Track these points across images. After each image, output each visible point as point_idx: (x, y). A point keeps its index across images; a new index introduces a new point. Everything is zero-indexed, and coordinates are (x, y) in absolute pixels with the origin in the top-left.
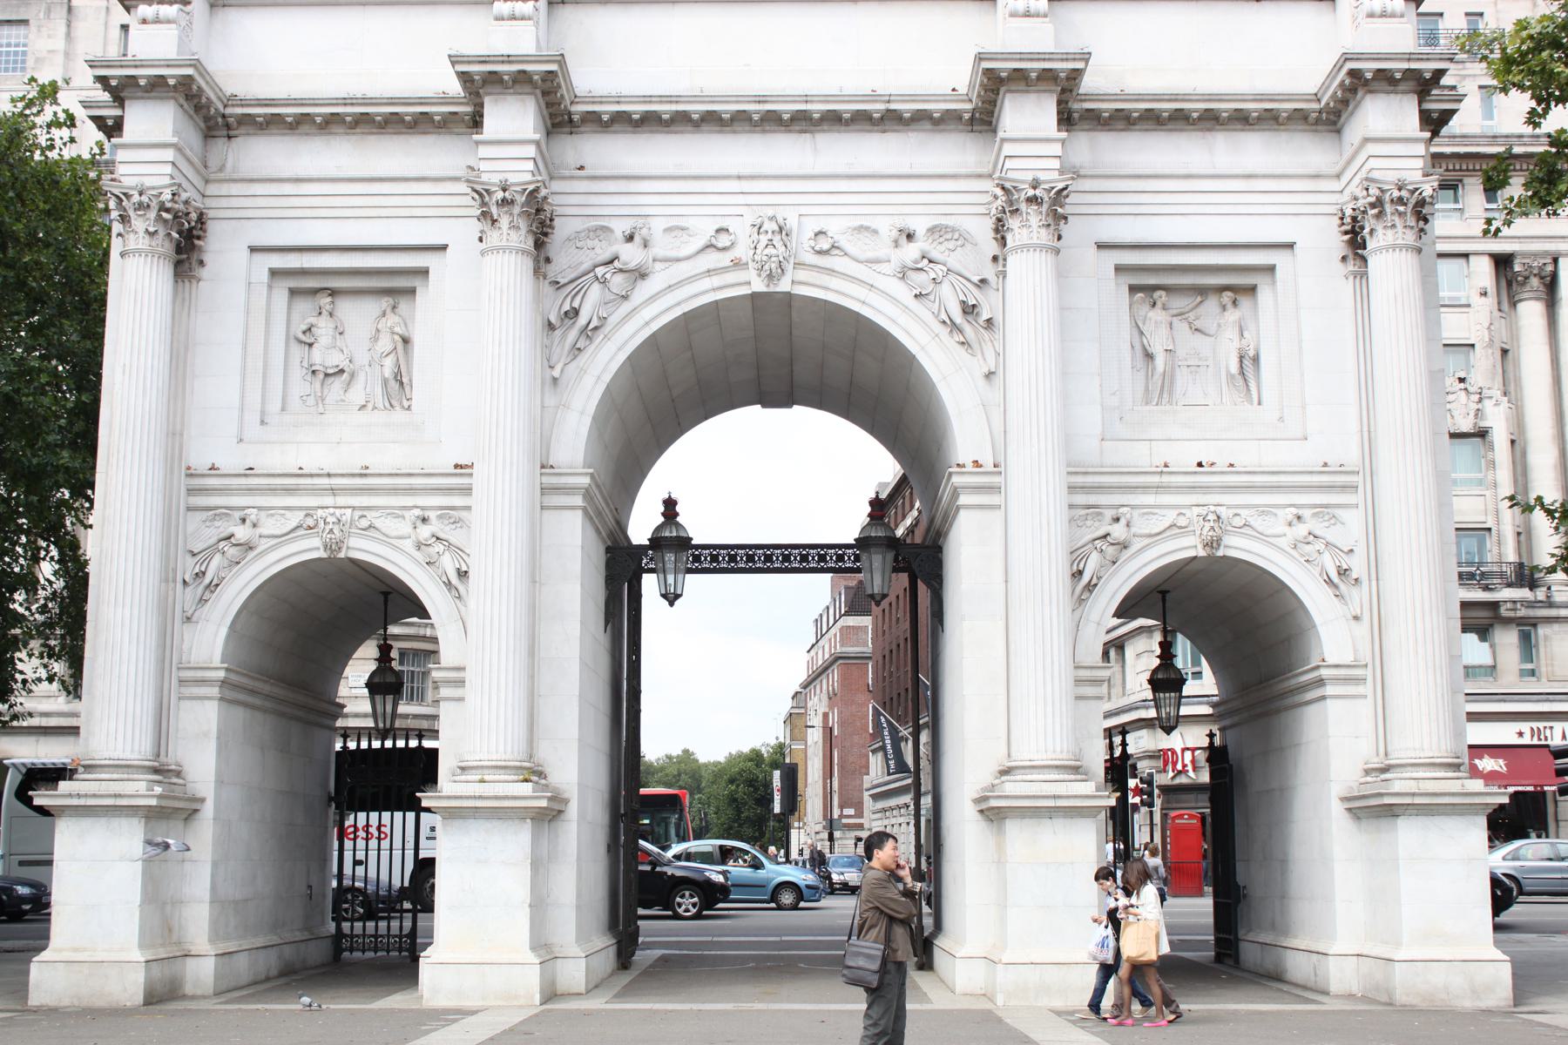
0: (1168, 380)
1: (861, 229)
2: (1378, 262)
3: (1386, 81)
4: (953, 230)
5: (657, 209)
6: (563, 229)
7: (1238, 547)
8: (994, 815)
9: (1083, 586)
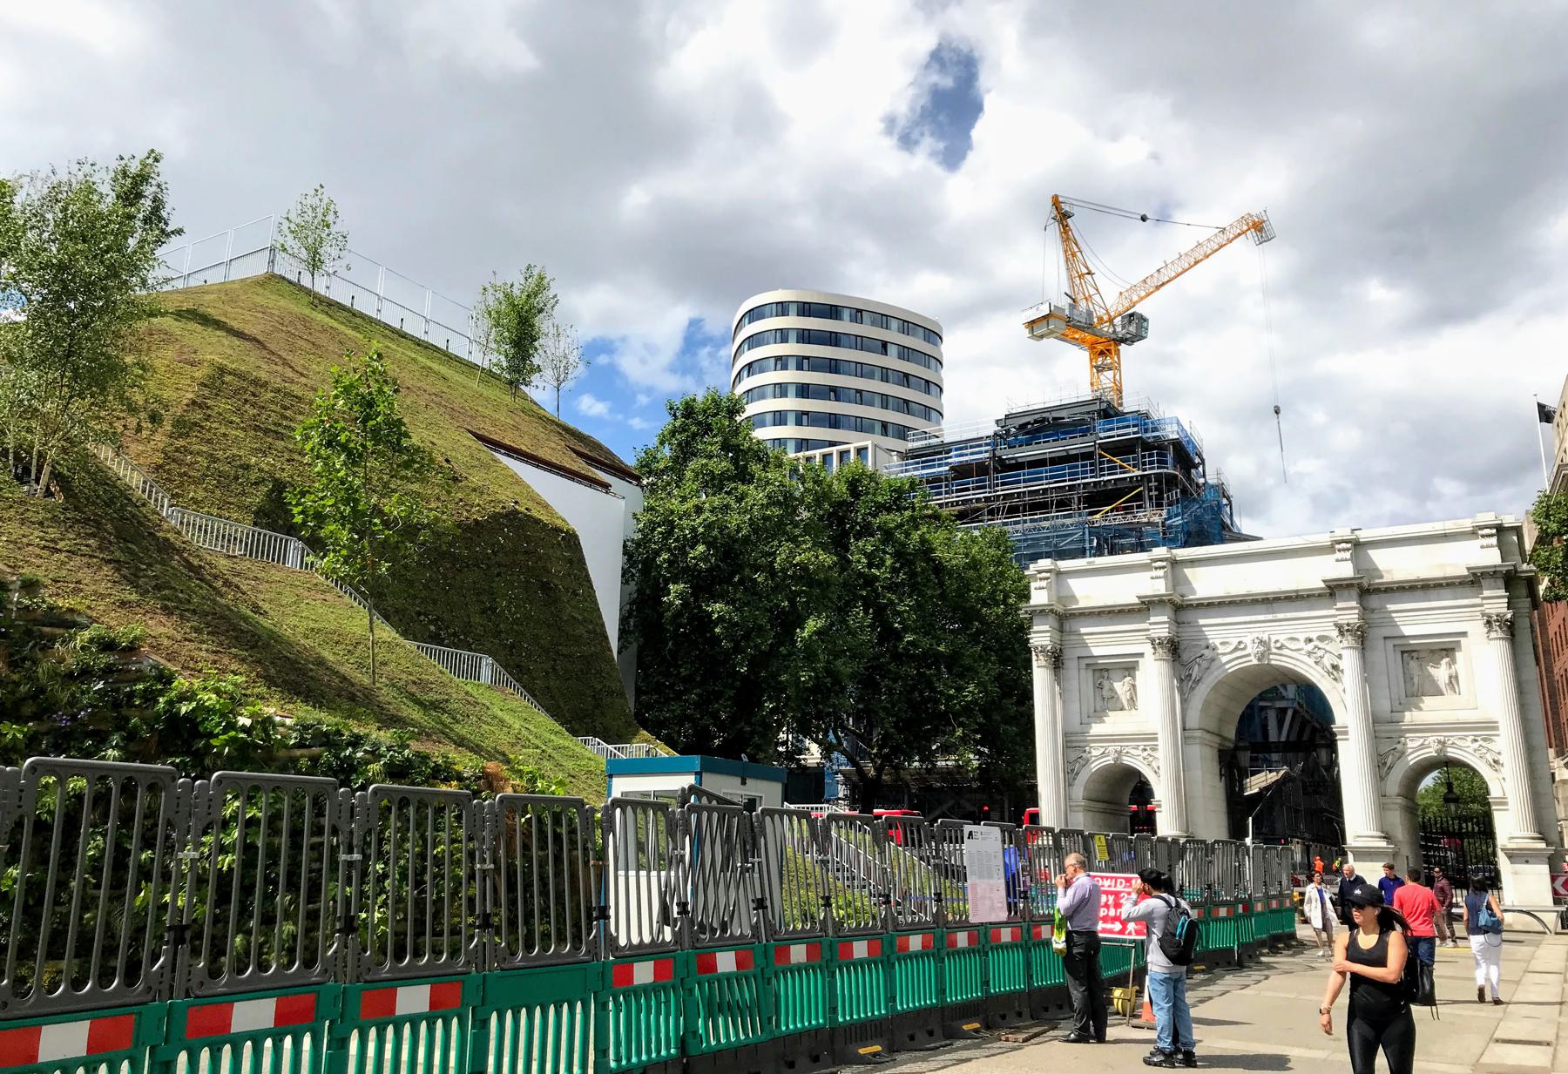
6: (1182, 647)
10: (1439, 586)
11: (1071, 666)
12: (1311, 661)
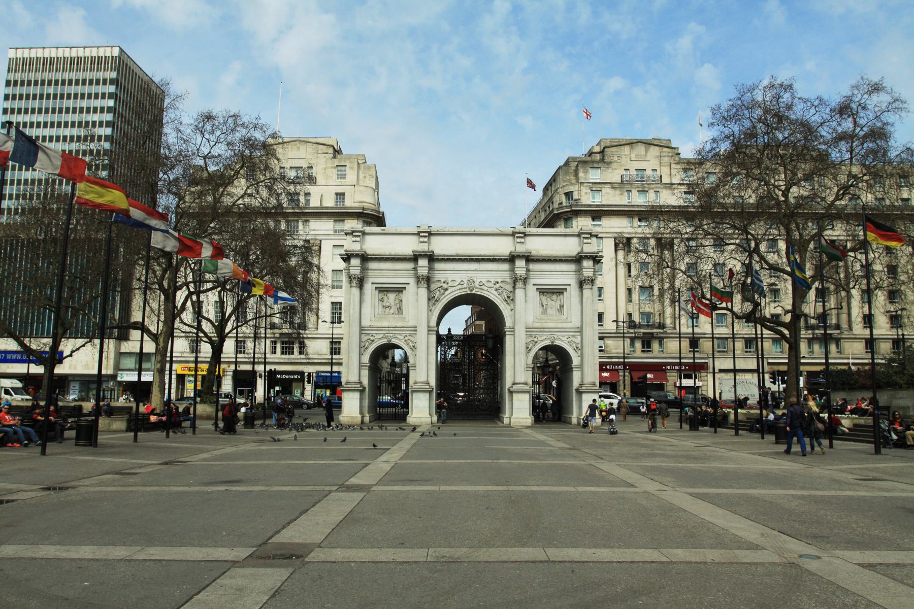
0: (546, 310)
2: (584, 291)
3: (587, 258)
5: (450, 276)
6: (432, 280)
7: (557, 343)
8: (511, 393)
9: (528, 350)
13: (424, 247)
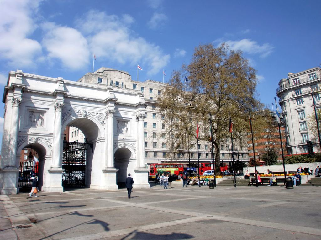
1: (93, 112)
4: (102, 113)
7: (127, 147)
10: (131, 106)
11: (24, 108)
12: (97, 119)
13: (62, 89)
